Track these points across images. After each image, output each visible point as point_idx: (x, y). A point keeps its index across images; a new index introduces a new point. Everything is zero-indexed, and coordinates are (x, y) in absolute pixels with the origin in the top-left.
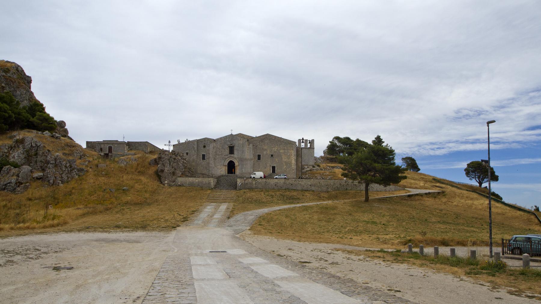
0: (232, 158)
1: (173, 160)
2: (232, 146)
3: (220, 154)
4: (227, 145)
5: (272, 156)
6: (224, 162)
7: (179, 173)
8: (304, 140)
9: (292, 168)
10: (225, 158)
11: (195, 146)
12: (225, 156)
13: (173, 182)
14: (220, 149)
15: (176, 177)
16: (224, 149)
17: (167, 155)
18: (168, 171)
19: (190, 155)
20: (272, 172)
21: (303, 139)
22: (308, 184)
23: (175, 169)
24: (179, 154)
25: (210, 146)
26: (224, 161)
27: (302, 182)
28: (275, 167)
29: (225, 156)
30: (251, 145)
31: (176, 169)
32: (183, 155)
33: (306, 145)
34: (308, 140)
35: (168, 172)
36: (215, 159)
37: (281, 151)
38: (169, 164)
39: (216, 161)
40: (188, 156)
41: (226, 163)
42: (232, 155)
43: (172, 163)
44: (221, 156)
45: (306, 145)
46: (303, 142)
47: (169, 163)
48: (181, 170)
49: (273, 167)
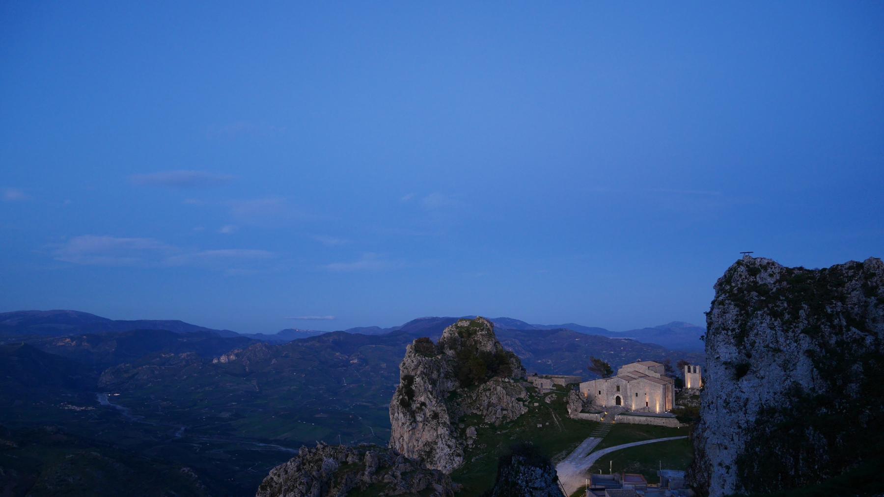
36: (607, 394)
42: (619, 392)
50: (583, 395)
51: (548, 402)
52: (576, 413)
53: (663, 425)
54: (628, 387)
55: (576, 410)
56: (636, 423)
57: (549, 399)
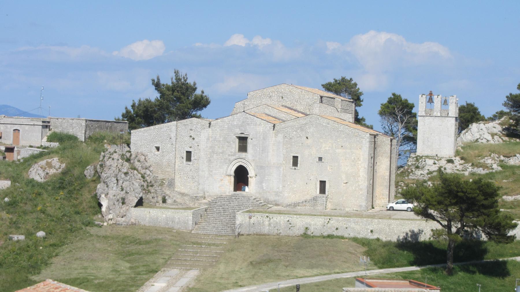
0: (243, 161)
1: (123, 176)
2: (243, 136)
3: (221, 151)
4: (234, 135)
5: (320, 159)
6: (227, 169)
7: (132, 200)
9: (359, 186)
10: (229, 160)
12: (229, 155)
13: (122, 217)
14: (220, 141)
15: (128, 207)
17: (115, 161)
18: (114, 196)
22: (367, 229)
25: (202, 135)
26: (228, 166)
27: (356, 225)
28: (325, 182)
29: (229, 155)
30: (280, 137)
31: (128, 193)
32: (145, 159)
35: (114, 198)
37: (337, 150)
38: (116, 184)
39: (211, 166)
42: (243, 155)
43: (120, 182)
44: (221, 155)
47: (116, 182)
48: (137, 195)
49: (321, 182)
50: (142, 158)
51: (38, 178)
52: (125, 208)
57: (41, 172)
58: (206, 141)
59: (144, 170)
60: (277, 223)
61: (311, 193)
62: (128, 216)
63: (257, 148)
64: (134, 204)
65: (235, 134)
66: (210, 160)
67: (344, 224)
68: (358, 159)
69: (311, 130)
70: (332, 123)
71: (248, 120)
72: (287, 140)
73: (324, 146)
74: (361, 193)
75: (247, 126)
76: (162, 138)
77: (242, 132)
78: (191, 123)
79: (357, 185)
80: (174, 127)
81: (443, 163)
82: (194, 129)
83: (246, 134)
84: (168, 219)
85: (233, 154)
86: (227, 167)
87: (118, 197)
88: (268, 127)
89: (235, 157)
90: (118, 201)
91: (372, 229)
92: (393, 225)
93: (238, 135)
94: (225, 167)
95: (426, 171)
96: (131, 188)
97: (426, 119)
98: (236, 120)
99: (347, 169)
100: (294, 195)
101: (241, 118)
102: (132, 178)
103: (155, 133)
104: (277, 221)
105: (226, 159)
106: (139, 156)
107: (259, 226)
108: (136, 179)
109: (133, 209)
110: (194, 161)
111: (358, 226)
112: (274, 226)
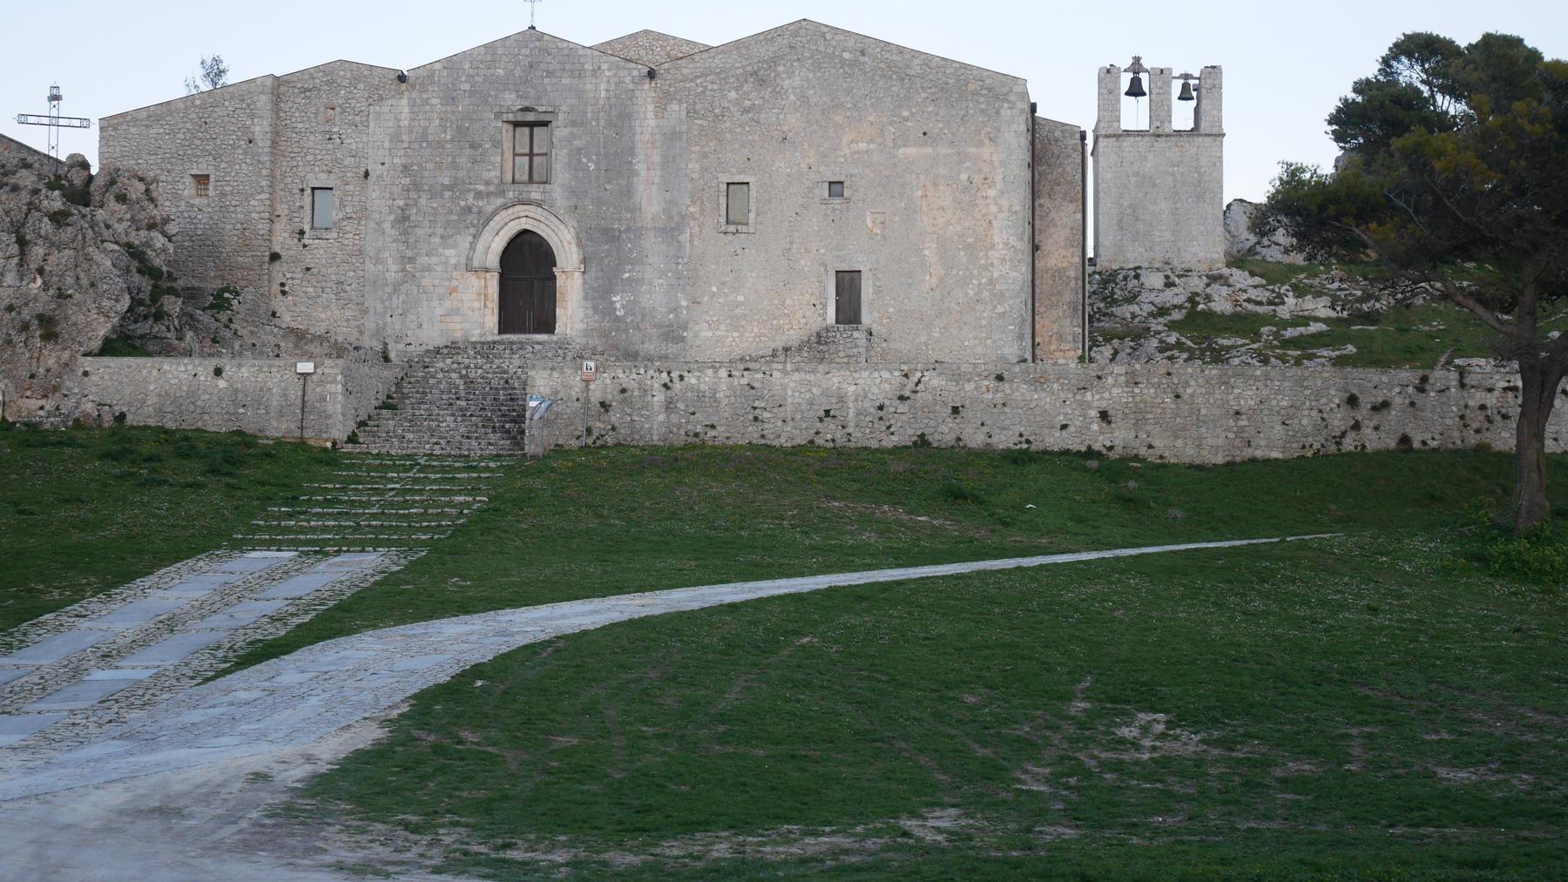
1: (47, 226)
2: (531, 117)
6: (472, 247)
8: (1144, 77)
9: (991, 281)
11: (261, 128)
12: (478, 195)
14: (440, 144)
15: (66, 355)
16: (473, 146)
19: (223, 194)
20: (838, 321)
21: (1136, 66)
23: (62, 296)
24: (115, 189)
25: (372, 124)
26: (476, 237)
29: (478, 195)
32: (147, 191)
33: (1160, 111)
34: (1176, 73)
36: (403, 219)
37: (901, 151)
38: (16, 260)
40: (204, 201)
41: (494, 244)
42: (535, 193)
43: (38, 251)
44: (447, 194)
45: (1160, 111)
46: (1135, 90)
47: (15, 249)
48: (106, 303)
52: (52, 358)
53: (1099, 438)
54: (647, 121)
55: (49, 328)
56: (788, 435)
58: (387, 145)
59: (143, 233)
60: (701, 396)
61: (803, 321)
62: (69, 389)
63: (584, 160)
64: (96, 344)
65: (498, 115)
66: (405, 218)
67: (984, 389)
68: (986, 179)
69: (797, 81)
70: (878, 50)
71: (549, 59)
72: (705, 124)
73: (845, 139)
74: (1000, 309)
75: (546, 81)
76: (218, 142)
77: (527, 104)
78: (327, 83)
79: (984, 281)
80: (263, 98)
81: (1196, 284)
82: (341, 102)
83: (544, 109)
84: (240, 396)
85: (492, 188)
86: (470, 239)
87: (26, 314)
88: (628, 80)
89: (500, 201)
90: (25, 327)
91: (1104, 405)
92: (1193, 383)
93: (511, 117)
94: (464, 241)
95: (1148, 308)
96: (82, 275)
97: (1124, 144)
98: (504, 58)
99: (941, 221)
100: (735, 334)
101: (523, 51)
102: (84, 238)
103: (189, 125)
104: (703, 387)
105: (469, 209)
106: (123, 180)
107: (629, 411)
108: (103, 242)
109: (88, 363)
110: (345, 223)
111: (1043, 395)
112: (691, 410)
